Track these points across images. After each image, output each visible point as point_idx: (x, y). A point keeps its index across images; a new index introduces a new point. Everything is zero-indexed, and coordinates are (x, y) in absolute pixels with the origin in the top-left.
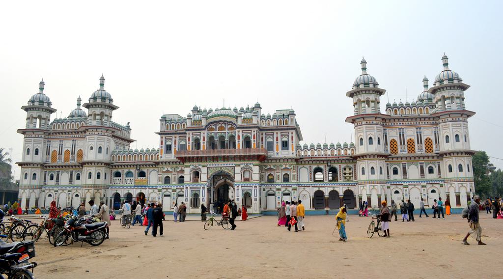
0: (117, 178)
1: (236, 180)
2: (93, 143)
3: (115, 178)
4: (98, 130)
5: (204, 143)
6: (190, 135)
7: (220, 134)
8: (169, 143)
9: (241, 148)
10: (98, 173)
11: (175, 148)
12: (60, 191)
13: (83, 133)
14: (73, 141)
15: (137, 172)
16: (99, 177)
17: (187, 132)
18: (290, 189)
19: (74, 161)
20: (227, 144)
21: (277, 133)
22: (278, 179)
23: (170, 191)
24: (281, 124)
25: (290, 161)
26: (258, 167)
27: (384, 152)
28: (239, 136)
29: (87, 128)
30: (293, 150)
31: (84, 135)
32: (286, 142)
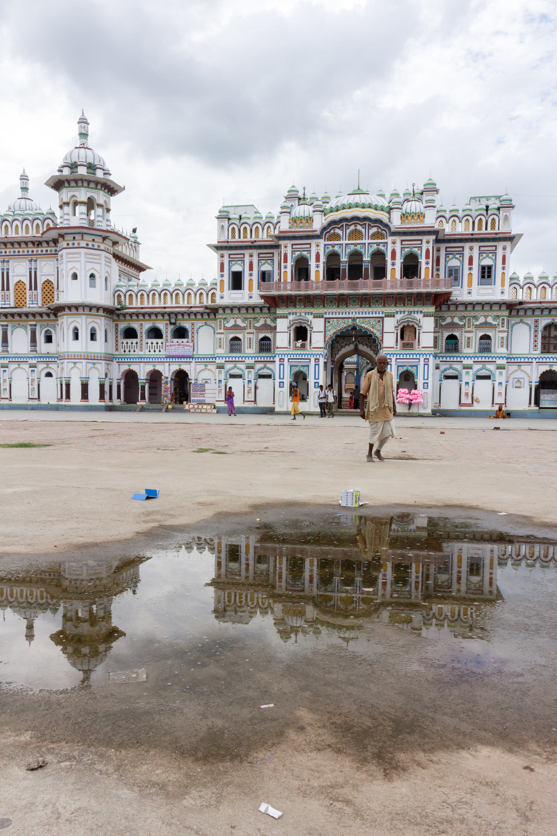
0: (130, 341)
1: (385, 344)
2: (76, 265)
3: (125, 341)
4: (86, 237)
5: (318, 266)
6: (287, 248)
7: (352, 247)
8: (237, 268)
9: (398, 275)
11: (250, 278)
12: (12, 366)
13: (52, 244)
14: (31, 261)
15: (171, 328)
16: (93, 337)
17: (282, 243)
19: (34, 302)
20: (367, 269)
21: (471, 249)
22: (468, 347)
23: (242, 366)
24: (480, 228)
25: (496, 307)
26: (432, 319)
28: (394, 253)
29: (62, 232)
30: (503, 285)
31: (53, 249)
32: (490, 267)
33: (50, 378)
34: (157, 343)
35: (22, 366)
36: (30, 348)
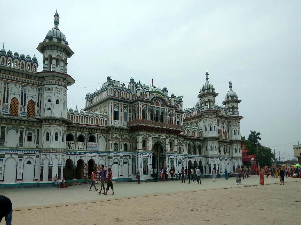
8: (116, 110)
10: (47, 134)
11: (121, 115)
13: (37, 78)
18: (181, 159)
27: (240, 139)
31: (37, 82)
33: (30, 165)
34: (80, 144)
35: (14, 156)
36: (18, 144)
